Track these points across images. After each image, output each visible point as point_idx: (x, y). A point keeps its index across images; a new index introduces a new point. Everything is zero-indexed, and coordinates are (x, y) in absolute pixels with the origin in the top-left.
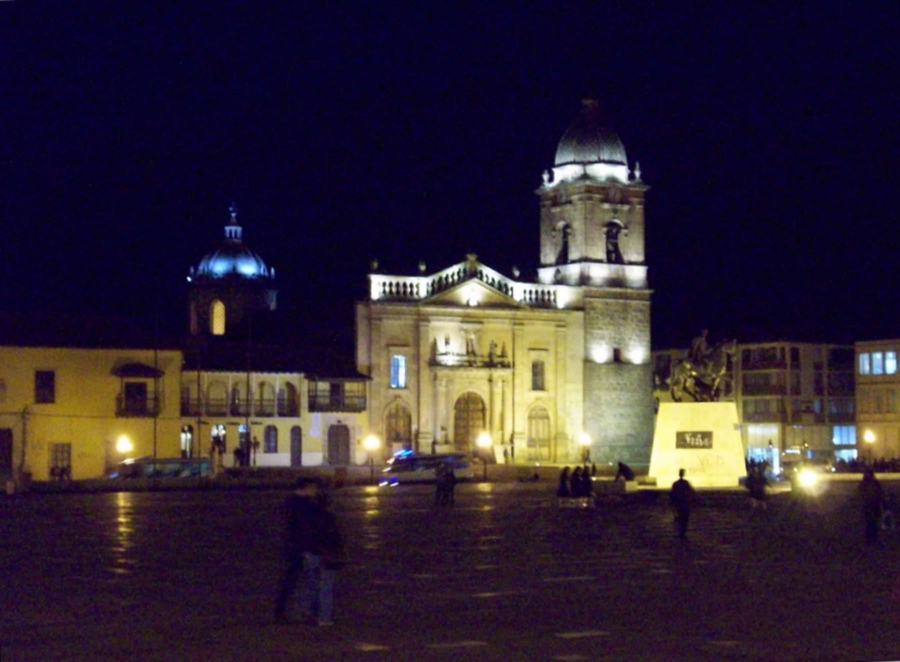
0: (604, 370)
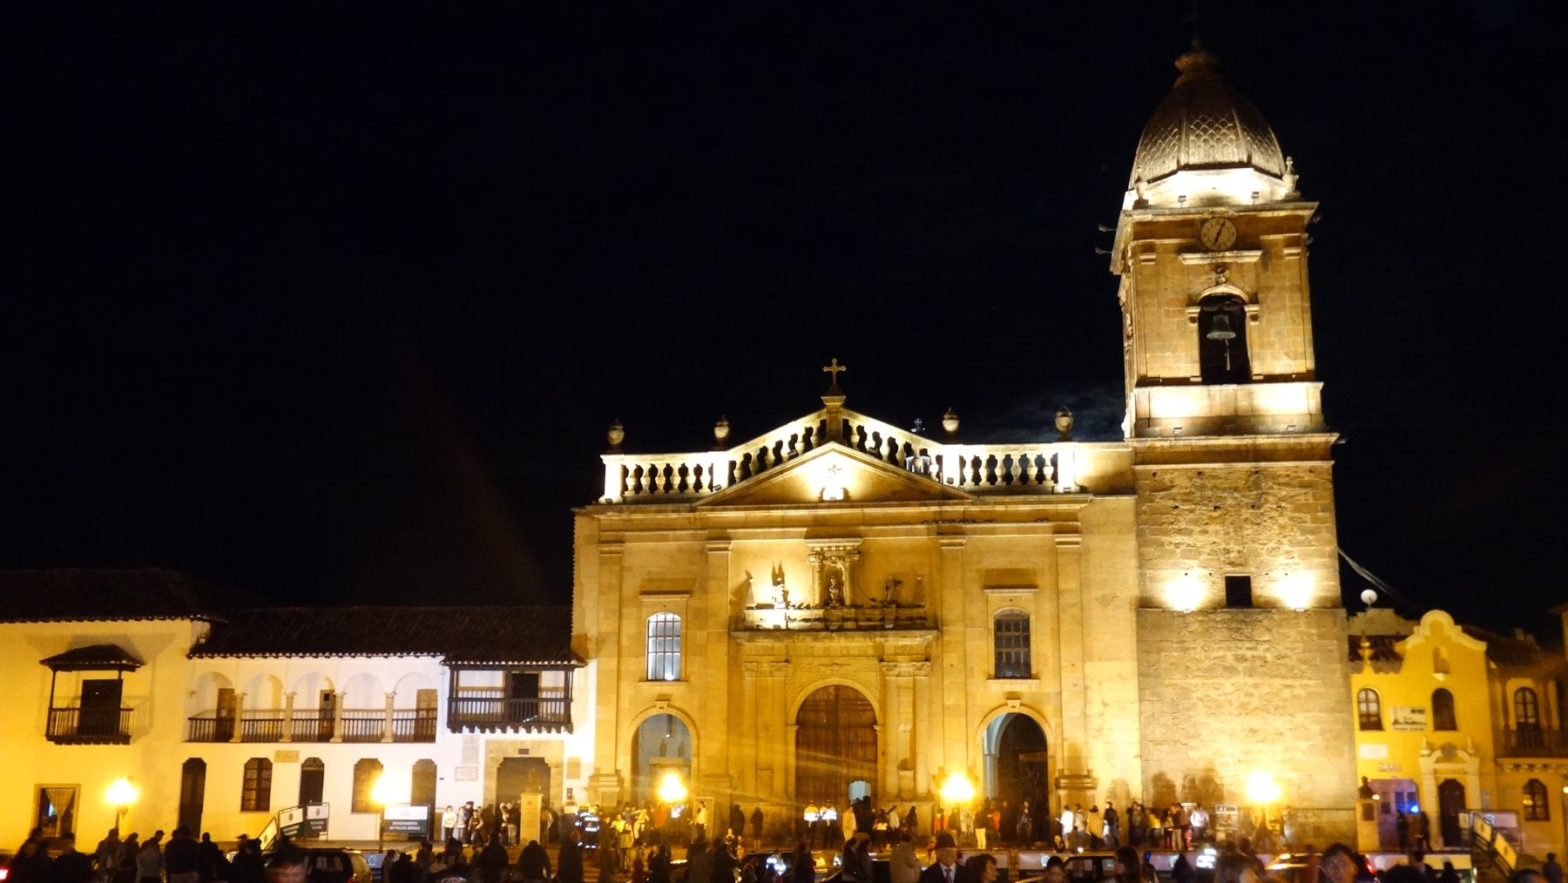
0: (1195, 627)
